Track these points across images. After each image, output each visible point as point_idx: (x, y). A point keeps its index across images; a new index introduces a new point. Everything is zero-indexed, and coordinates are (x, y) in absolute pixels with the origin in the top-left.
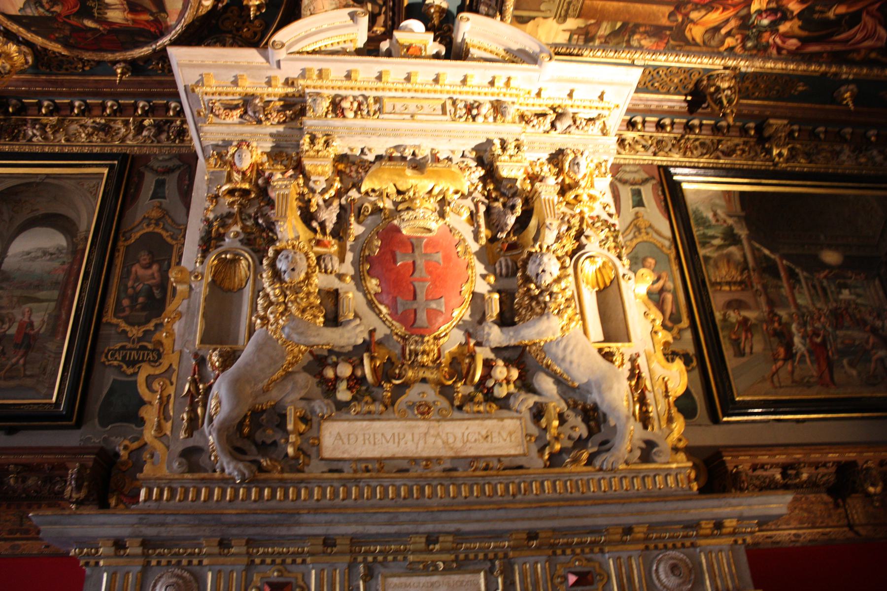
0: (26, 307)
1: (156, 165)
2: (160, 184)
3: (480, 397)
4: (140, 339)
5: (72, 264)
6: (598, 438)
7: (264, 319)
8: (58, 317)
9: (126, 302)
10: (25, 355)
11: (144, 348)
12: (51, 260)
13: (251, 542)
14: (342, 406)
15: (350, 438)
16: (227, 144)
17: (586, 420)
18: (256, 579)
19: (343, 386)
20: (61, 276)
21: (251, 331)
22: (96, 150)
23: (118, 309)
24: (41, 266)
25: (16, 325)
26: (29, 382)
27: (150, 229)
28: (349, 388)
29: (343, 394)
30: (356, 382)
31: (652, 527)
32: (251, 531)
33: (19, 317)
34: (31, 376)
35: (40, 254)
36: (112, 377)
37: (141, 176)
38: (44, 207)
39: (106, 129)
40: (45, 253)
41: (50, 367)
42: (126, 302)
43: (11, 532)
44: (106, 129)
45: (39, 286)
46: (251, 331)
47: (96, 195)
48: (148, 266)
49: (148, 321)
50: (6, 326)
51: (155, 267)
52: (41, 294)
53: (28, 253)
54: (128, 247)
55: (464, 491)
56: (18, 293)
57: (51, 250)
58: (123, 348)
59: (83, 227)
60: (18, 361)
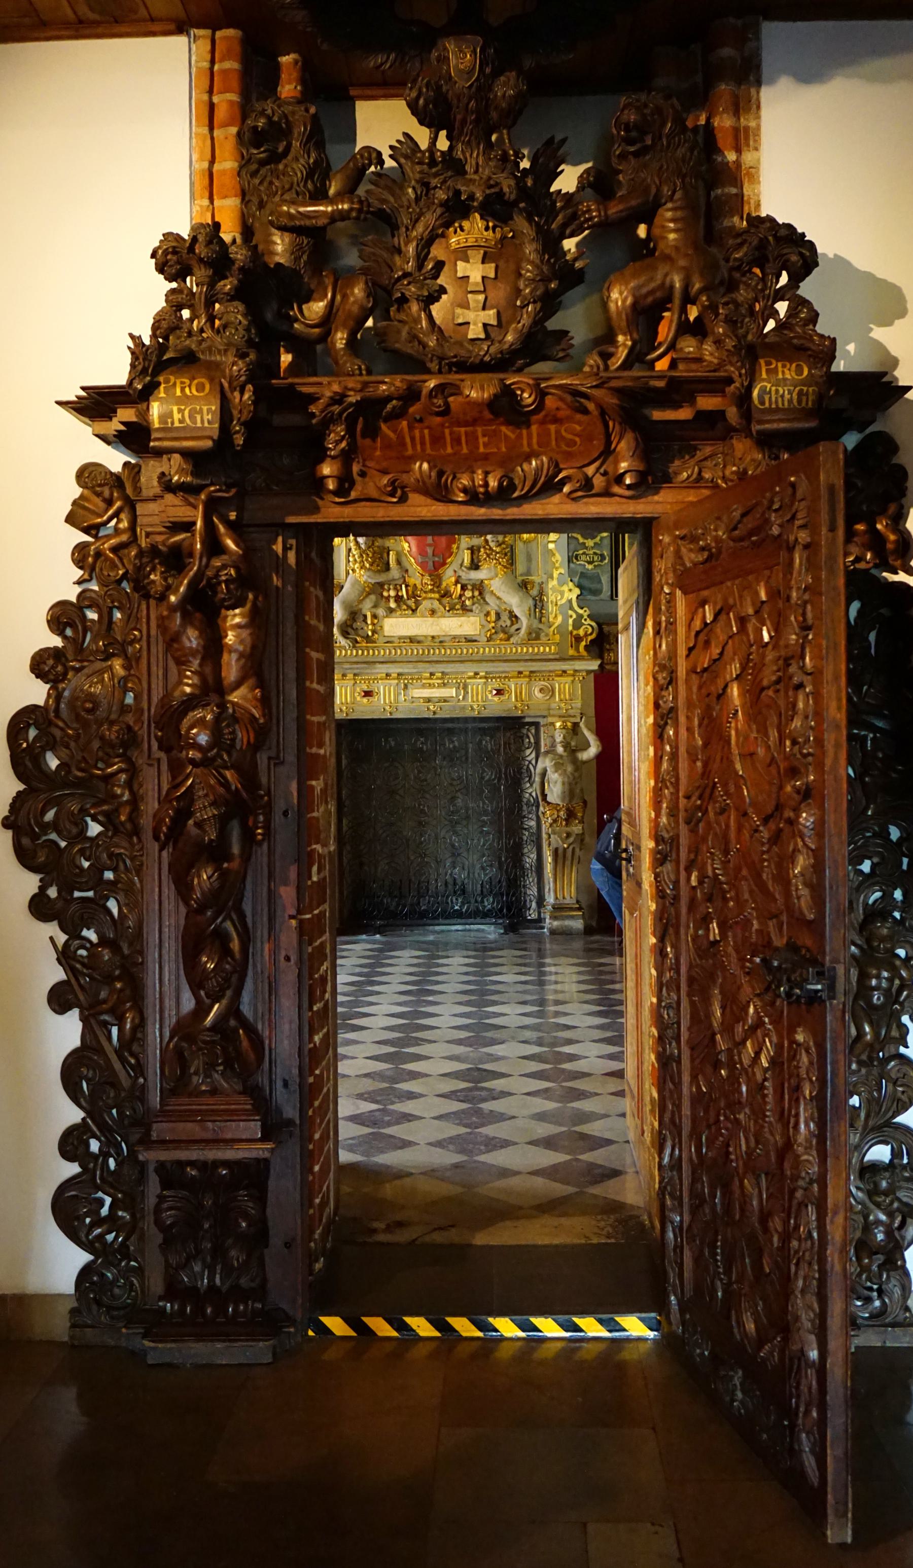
3: (458, 607)
6: (515, 627)
7: (354, 570)
13: (355, 675)
14: (391, 611)
15: (397, 626)
17: (510, 618)
18: (358, 689)
19: (392, 600)
21: (348, 573)
28: (396, 601)
29: (393, 605)
30: (398, 599)
31: (531, 672)
32: (356, 671)
46: (348, 573)
55: (448, 652)
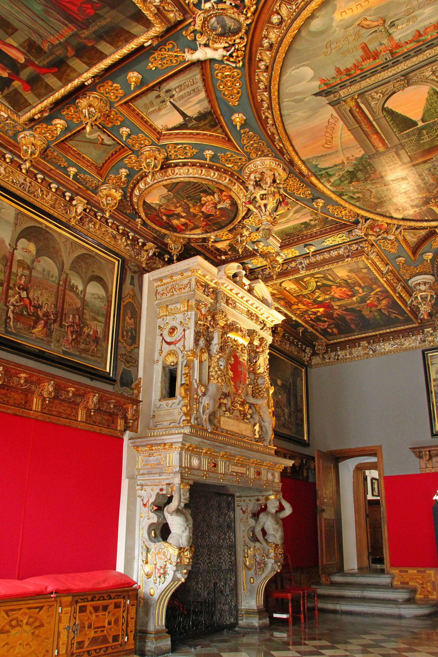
0: (96, 322)
1: (131, 267)
2: (132, 278)
4: (130, 352)
5: (108, 306)
8: (105, 332)
9: (125, 333)
10: (96, 346)
11: (131, 357)
12: (101, 301)
16: (200, 301)
20: (105, 312)
22: (111, 247)
23: (123, 336)
24: (100, 304)
25: (92, 330)
26: (99, 360)
27: (130, 300)
33: (93, 327)
34: (99, 357)
35: (97, 297)
36: (123, 366)
37: (126, 271)
38: (97, 273)
39: (115, 237)
40: (99, 297)
41: (104, 355)
42: (125, 333)
43: (99, 423)
44: (115, 237)
45: (98, 314)
47: (113, 273)
48: (130, 319)
49: (131, 345)
50: (89, 329)
51: (133, 320)
52: (99, 318)
53: (93, 295)
54: (124, 306)
56: (92, 314)
57: (101, 297)
58: (125, 354)
59: (110, 290)
60: (94, 349)
